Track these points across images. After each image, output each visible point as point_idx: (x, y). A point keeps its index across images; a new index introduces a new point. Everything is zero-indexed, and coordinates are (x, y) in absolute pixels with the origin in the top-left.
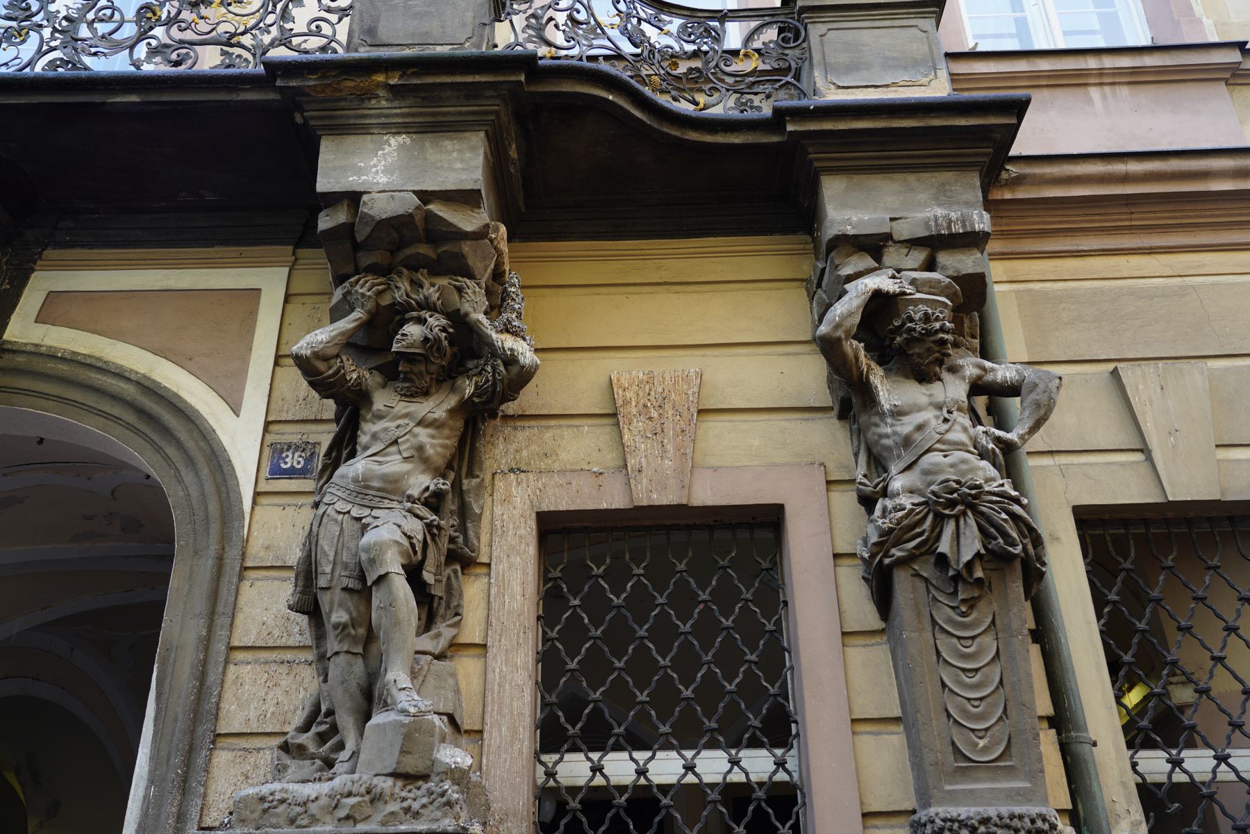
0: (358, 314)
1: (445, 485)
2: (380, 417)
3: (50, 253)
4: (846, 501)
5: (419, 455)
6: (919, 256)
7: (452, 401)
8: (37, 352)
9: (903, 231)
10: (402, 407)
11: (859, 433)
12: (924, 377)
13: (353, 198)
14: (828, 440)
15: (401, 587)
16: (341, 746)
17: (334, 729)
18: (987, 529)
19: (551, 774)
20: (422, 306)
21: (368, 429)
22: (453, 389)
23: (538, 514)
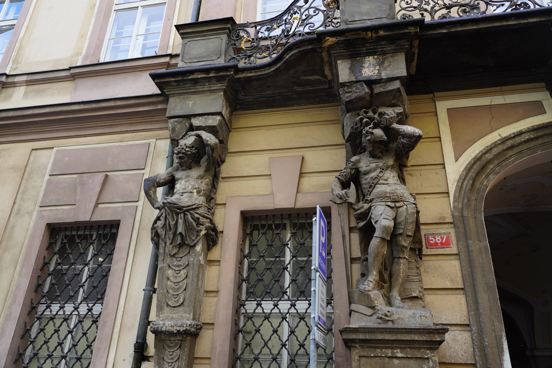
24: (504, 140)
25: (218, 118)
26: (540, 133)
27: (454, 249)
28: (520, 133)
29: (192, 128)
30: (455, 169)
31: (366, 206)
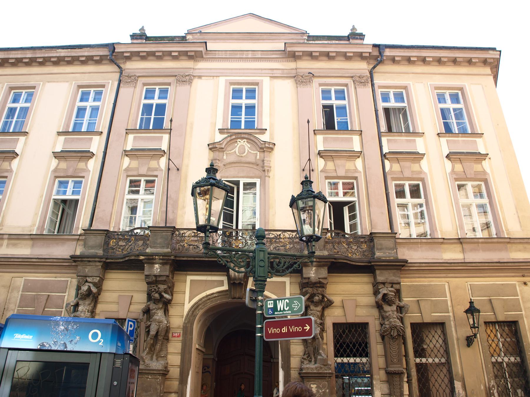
2: (311, 310)
6: (391, 285)
7: (321, 307)
9: (388, 281)
10: (315, 309)
11: (380, 312)
12: (390, 305)
13: (309, 278)
14: (375, 312)
17: (309, 356)
18: (398, 331)
20: (319, 294)
23: (333, 323)
24: (207, 296)
25: (98, 278)
26: (220, 294)
27: (181, 338)
28: (213, 294)
29: (87, 281)
30: (188, 306)
31: (149, 323)
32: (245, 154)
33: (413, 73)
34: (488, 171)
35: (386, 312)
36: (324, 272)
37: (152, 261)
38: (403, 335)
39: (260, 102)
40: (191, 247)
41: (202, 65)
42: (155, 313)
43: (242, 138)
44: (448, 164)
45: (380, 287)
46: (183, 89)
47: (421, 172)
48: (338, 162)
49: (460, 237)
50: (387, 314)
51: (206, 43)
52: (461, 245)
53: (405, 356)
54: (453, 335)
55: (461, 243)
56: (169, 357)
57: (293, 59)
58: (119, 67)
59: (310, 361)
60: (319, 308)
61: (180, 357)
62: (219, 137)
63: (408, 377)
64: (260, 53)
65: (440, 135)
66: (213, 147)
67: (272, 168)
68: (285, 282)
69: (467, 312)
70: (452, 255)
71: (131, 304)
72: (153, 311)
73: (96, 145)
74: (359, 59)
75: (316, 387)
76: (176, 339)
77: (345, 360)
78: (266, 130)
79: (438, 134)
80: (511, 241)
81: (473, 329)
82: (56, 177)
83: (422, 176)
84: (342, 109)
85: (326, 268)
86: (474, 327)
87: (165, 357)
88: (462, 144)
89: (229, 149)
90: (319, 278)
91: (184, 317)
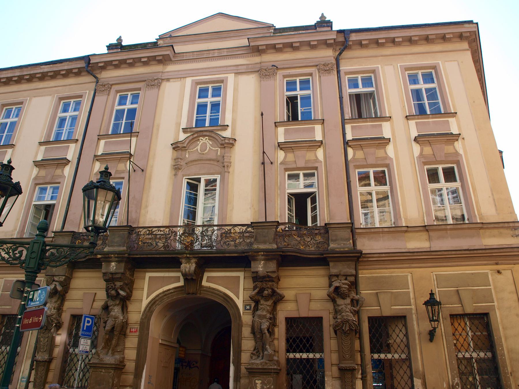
0: (258, 289)
1: (271, 316)
2: (261, 305)
3: (206, 269)
4: (331, 316)
5: (268, 311)
6: (344, 278)
7: (272, 301)
8: (207, 287)
9: (342, 273)
10: (265, 303)
11: (334, 306)
12: (344, 299)
13: (257, 272)
14: (330, 306)
15: (267, 334)
16: (260, 354)
17: (258, 351)
18: (350, 325)
19: (288, 357)
20: (268, 288)
21: (260, 307)
22: (272, 299)
24: (164, 292)
25: (64, 277)
26: (178, 290)
27: (138, 334)
28: (169, 290)
29: (54, 281)
30: (145, 302)
31: (106, 319)
32: (206, 151)
33: (382, 56)
34: (461, 152)
35: (338, 305)
36: (272, 266)
37: (109, 259)
38: (356, 330)
39: (225, 100)
40: (146, 244)
41: (171, 68)
42: (112, 309)
43: (204, 136)
44: (416, 149)
45: (333, 280)
46: (152, 92)
47: (387, 157)
48: (299, 153)
49: (426, 224)
50: (340, 308)
51: (172, 46)
52: (427, 233)
53: (360, 351)
54: (414, 329)
55: (427, 230)
56: (126, 351)
57: (258, 53)
58: (96, 77)
59: (259, 356)
60: (270, 303)
61: (136, 351)
62: (182, 136)
63: (362, 374)
64: (225, 50)
65: (408, 117)
66: (176, 146)
67: (232, 164)
68: (239, 277)
69: (426, 303)
70: (417, 243)
71: (94, 301)
72: (111, 308)
73: (71, 152)
74: (325, 47)
75: (261, 383)
76: (133, 334)
77: (298, 356)
78: (228, 126)
79: (406, 117)
80: (485, 226)
81: (433, 323)
82: (37, 184)
83: (387, 162)
84: (306, 99)
85: (275, 261)
86: (434, 321)
87: (122, 351)
88: (432, 125)
89: (191, 147)
90: (267, 272)
91: (142, 313)
